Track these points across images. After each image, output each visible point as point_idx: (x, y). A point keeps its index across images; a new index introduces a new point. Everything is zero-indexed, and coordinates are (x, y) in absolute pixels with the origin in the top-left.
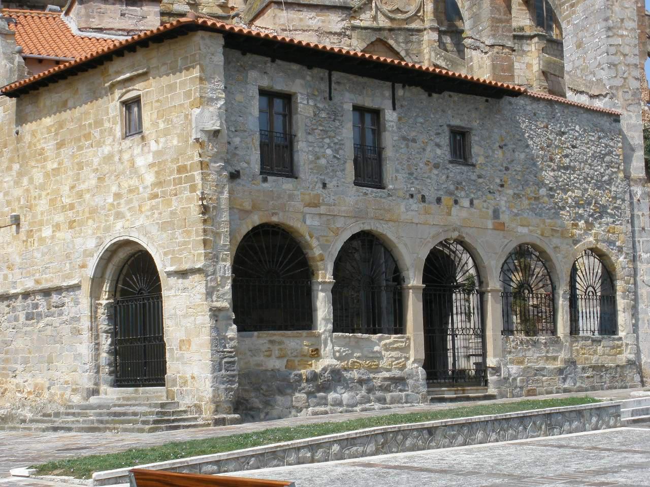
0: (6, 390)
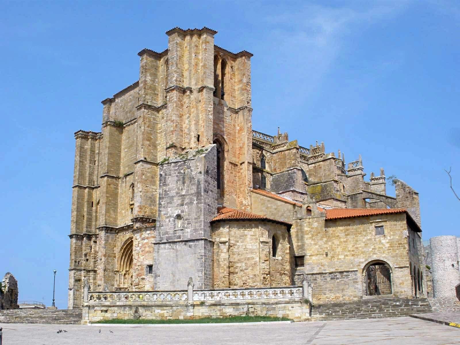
0: (320, 298)
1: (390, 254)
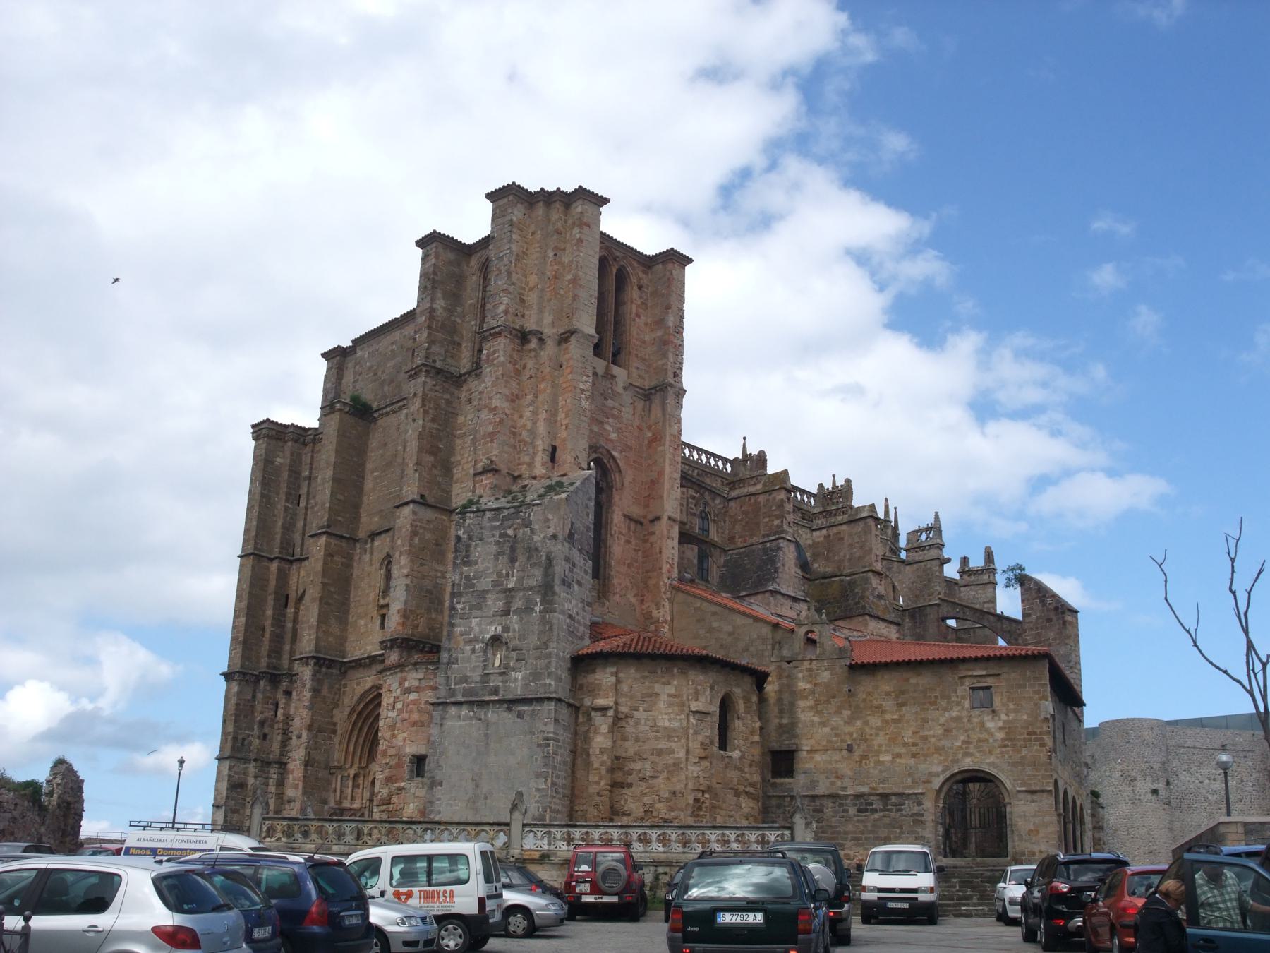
1: (1006, 756)
